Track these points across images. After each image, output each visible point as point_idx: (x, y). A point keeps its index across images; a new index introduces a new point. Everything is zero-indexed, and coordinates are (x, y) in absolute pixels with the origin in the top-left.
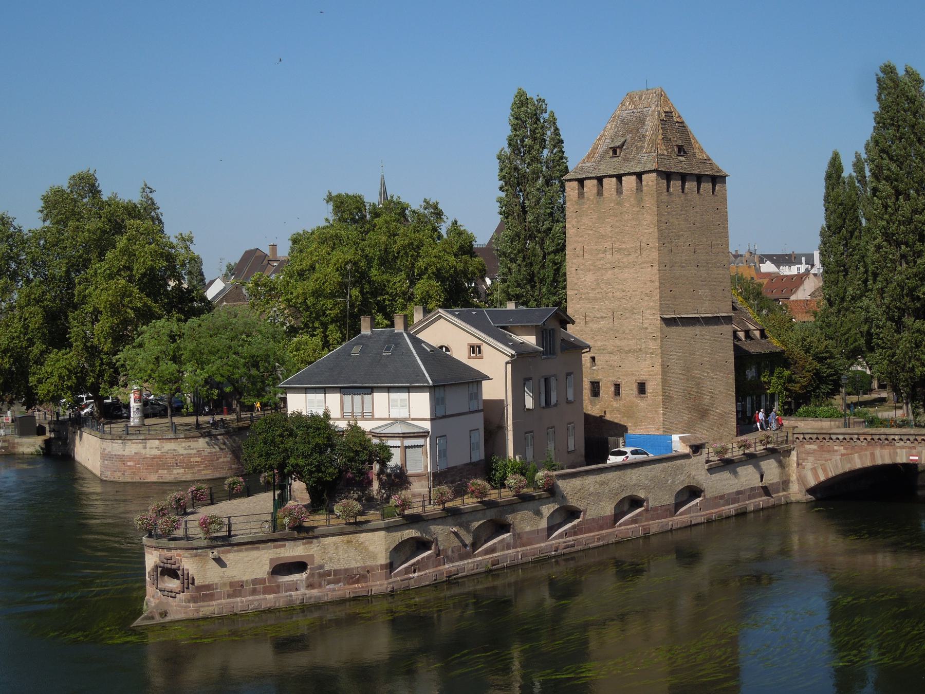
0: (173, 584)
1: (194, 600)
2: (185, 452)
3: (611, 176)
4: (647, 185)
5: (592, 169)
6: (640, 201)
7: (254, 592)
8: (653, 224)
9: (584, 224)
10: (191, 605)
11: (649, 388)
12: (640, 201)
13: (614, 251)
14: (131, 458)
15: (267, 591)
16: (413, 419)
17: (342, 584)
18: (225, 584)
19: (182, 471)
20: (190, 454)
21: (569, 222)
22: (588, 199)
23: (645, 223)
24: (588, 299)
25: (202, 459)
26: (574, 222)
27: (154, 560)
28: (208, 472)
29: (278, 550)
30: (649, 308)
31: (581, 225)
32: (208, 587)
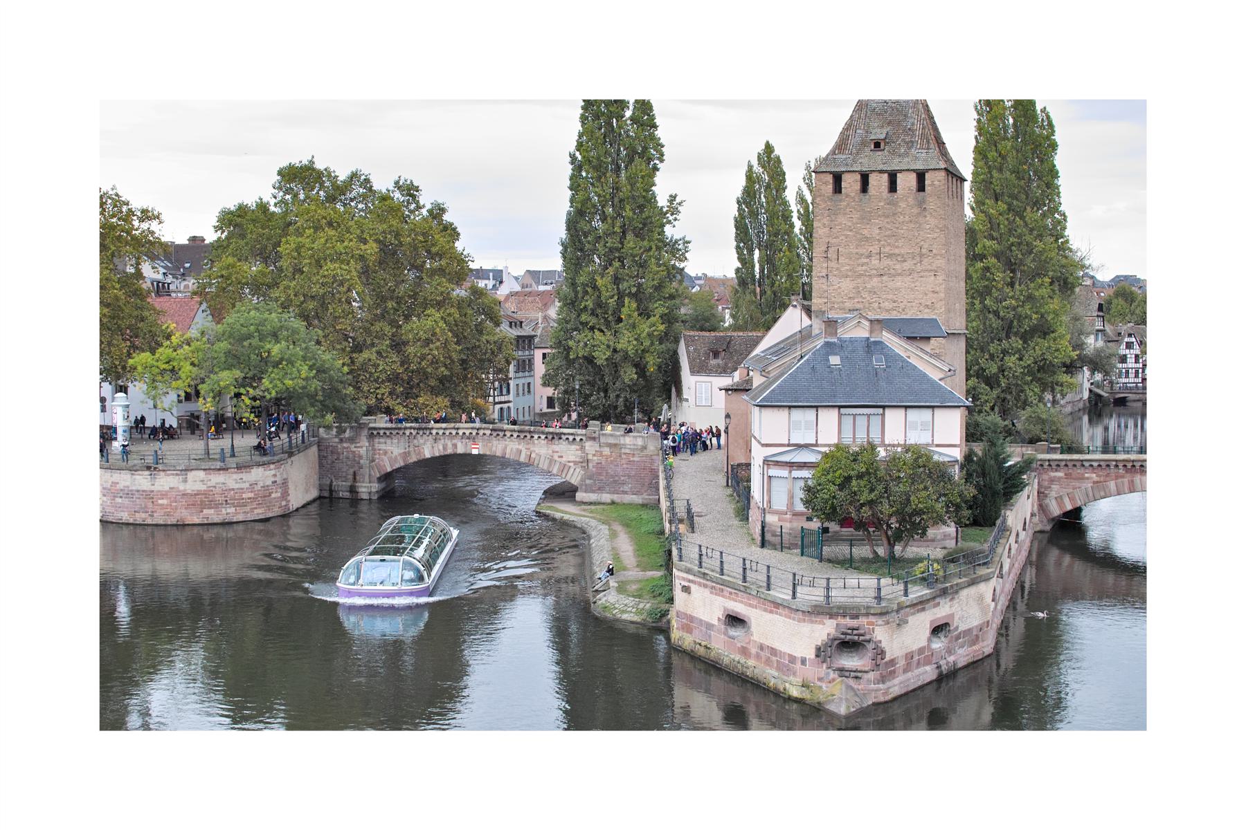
0: (851, 661)
1: (883, 679)
2: (237, 486)
3: (881, 172)
4: (932, 185)
5: (849, 161)
6: (921, 204)
8: (938, 228)
10: (881, 686)
12: (921, 204)
13: (882, 256)
14: (164, 495)
15: (928, 661)
16: (938, 446)
18: (902, 656)
19: (233, 510)
20: (242, 489)
21: (819, 220)
22: (847, 196)
23: (928, 227)
24: (844, 309)
25: (255, 495)
26: (826, 221)
27: (827, 632)
28: (260, 511)
31: (835, 225)
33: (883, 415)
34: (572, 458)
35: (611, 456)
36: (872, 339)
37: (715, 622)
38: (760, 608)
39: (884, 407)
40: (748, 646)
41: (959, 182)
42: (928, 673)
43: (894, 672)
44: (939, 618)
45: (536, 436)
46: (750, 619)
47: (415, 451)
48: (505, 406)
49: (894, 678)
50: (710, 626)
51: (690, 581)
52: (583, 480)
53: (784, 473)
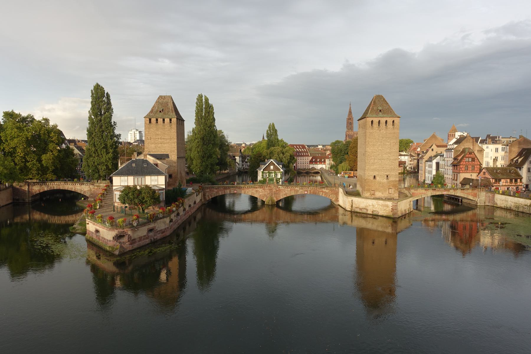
5: (153, 115)
6: (171, 126)
7: (144, 239)
10: (131, 246)
11: (173, 176)
12: (171, 126)
15: (147, 238)
16: (159, 185)
17: (160, 234)
26: (148, 130)
29: (149, 226)
30: (173, 155)
32: (134, 239)
33: (145, 178)
35: (97, 189)
36: (144, 159)
37: (94, 232)
39: (145, 176)
41: (182, 121)
42: (147, 241)
43: (135, 242)
44: (150, 228)
45: (77, 184)
48: (84, 176)
49: (135, 243)
50: (93, 233)
51: (89, 221)
52: (90, 195)
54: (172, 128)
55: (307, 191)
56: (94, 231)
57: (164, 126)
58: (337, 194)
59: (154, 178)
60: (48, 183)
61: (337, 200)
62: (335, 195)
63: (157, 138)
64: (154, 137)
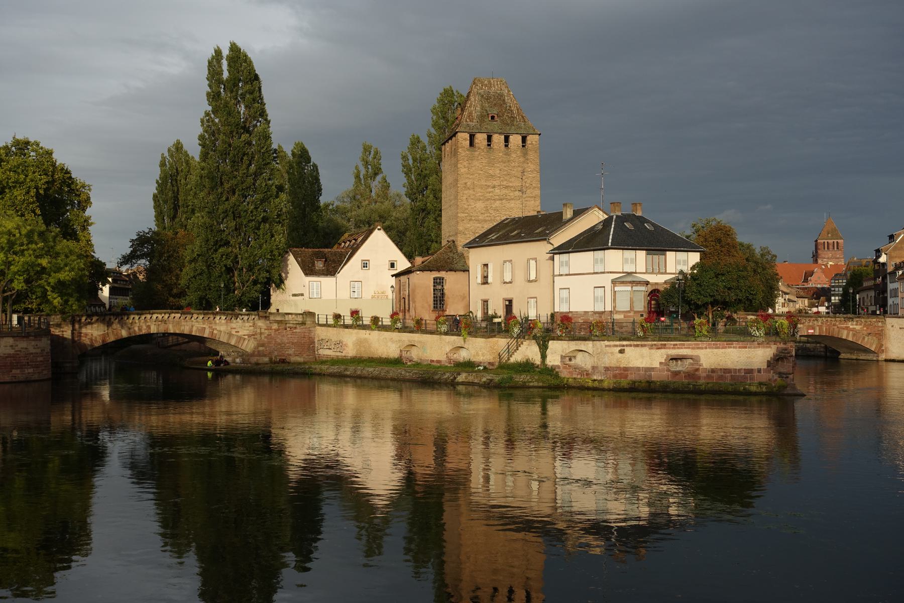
2: (34, 351)
6: (525, 154)
9: (475, 166)
12: (525, 154)
19: (31, 370)
20: (37, 353)
22: (479, 148)
23: (529, 170)
24: (478, 220)
33: (665, 255)
34: (246, 332)
35: (278, 330)
37: (658, 366)
38: (710, 348)
40: (697, 373)
46: (698, 356)
47: (113, 332)
53: (629, 288)
54: (527, 159)
55: (813, 328)
56: (661, 363)
57: (509, 155)
58: (880, 335)
59: (682, 256)
60: (157, 313)
61: (881, 349)
62: (875, 338)
63: (489, 186)
64: (483, 183)
